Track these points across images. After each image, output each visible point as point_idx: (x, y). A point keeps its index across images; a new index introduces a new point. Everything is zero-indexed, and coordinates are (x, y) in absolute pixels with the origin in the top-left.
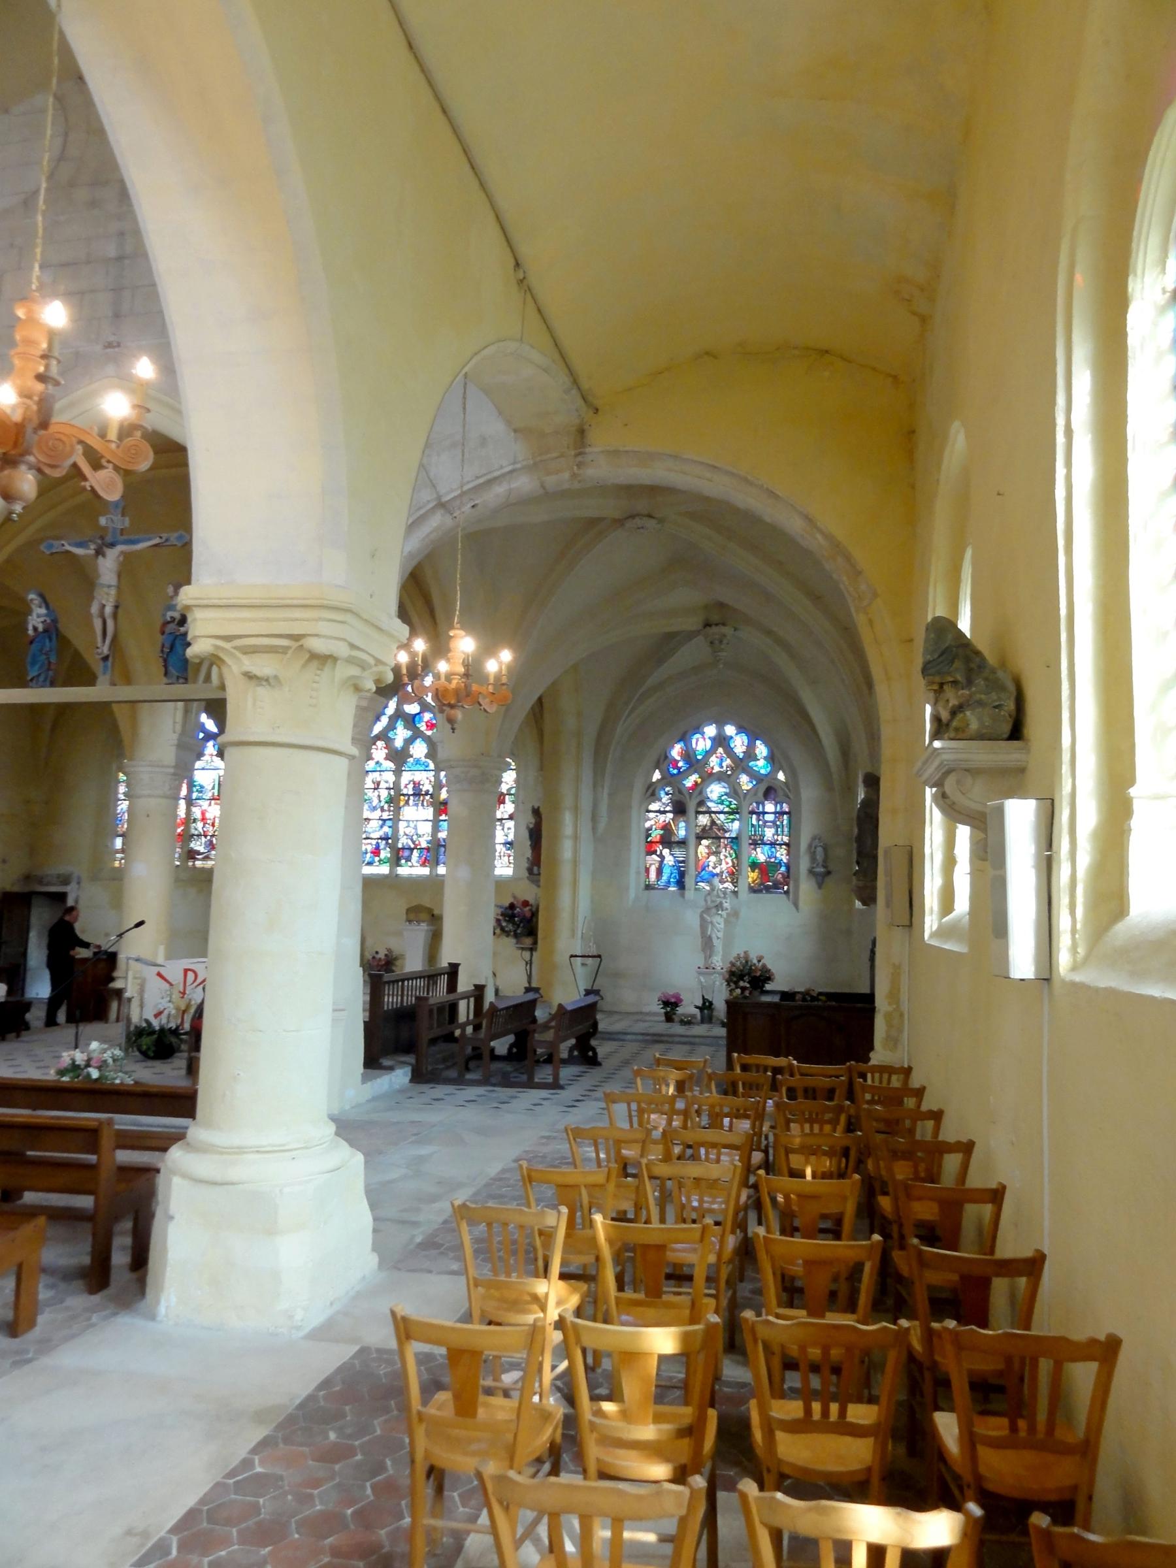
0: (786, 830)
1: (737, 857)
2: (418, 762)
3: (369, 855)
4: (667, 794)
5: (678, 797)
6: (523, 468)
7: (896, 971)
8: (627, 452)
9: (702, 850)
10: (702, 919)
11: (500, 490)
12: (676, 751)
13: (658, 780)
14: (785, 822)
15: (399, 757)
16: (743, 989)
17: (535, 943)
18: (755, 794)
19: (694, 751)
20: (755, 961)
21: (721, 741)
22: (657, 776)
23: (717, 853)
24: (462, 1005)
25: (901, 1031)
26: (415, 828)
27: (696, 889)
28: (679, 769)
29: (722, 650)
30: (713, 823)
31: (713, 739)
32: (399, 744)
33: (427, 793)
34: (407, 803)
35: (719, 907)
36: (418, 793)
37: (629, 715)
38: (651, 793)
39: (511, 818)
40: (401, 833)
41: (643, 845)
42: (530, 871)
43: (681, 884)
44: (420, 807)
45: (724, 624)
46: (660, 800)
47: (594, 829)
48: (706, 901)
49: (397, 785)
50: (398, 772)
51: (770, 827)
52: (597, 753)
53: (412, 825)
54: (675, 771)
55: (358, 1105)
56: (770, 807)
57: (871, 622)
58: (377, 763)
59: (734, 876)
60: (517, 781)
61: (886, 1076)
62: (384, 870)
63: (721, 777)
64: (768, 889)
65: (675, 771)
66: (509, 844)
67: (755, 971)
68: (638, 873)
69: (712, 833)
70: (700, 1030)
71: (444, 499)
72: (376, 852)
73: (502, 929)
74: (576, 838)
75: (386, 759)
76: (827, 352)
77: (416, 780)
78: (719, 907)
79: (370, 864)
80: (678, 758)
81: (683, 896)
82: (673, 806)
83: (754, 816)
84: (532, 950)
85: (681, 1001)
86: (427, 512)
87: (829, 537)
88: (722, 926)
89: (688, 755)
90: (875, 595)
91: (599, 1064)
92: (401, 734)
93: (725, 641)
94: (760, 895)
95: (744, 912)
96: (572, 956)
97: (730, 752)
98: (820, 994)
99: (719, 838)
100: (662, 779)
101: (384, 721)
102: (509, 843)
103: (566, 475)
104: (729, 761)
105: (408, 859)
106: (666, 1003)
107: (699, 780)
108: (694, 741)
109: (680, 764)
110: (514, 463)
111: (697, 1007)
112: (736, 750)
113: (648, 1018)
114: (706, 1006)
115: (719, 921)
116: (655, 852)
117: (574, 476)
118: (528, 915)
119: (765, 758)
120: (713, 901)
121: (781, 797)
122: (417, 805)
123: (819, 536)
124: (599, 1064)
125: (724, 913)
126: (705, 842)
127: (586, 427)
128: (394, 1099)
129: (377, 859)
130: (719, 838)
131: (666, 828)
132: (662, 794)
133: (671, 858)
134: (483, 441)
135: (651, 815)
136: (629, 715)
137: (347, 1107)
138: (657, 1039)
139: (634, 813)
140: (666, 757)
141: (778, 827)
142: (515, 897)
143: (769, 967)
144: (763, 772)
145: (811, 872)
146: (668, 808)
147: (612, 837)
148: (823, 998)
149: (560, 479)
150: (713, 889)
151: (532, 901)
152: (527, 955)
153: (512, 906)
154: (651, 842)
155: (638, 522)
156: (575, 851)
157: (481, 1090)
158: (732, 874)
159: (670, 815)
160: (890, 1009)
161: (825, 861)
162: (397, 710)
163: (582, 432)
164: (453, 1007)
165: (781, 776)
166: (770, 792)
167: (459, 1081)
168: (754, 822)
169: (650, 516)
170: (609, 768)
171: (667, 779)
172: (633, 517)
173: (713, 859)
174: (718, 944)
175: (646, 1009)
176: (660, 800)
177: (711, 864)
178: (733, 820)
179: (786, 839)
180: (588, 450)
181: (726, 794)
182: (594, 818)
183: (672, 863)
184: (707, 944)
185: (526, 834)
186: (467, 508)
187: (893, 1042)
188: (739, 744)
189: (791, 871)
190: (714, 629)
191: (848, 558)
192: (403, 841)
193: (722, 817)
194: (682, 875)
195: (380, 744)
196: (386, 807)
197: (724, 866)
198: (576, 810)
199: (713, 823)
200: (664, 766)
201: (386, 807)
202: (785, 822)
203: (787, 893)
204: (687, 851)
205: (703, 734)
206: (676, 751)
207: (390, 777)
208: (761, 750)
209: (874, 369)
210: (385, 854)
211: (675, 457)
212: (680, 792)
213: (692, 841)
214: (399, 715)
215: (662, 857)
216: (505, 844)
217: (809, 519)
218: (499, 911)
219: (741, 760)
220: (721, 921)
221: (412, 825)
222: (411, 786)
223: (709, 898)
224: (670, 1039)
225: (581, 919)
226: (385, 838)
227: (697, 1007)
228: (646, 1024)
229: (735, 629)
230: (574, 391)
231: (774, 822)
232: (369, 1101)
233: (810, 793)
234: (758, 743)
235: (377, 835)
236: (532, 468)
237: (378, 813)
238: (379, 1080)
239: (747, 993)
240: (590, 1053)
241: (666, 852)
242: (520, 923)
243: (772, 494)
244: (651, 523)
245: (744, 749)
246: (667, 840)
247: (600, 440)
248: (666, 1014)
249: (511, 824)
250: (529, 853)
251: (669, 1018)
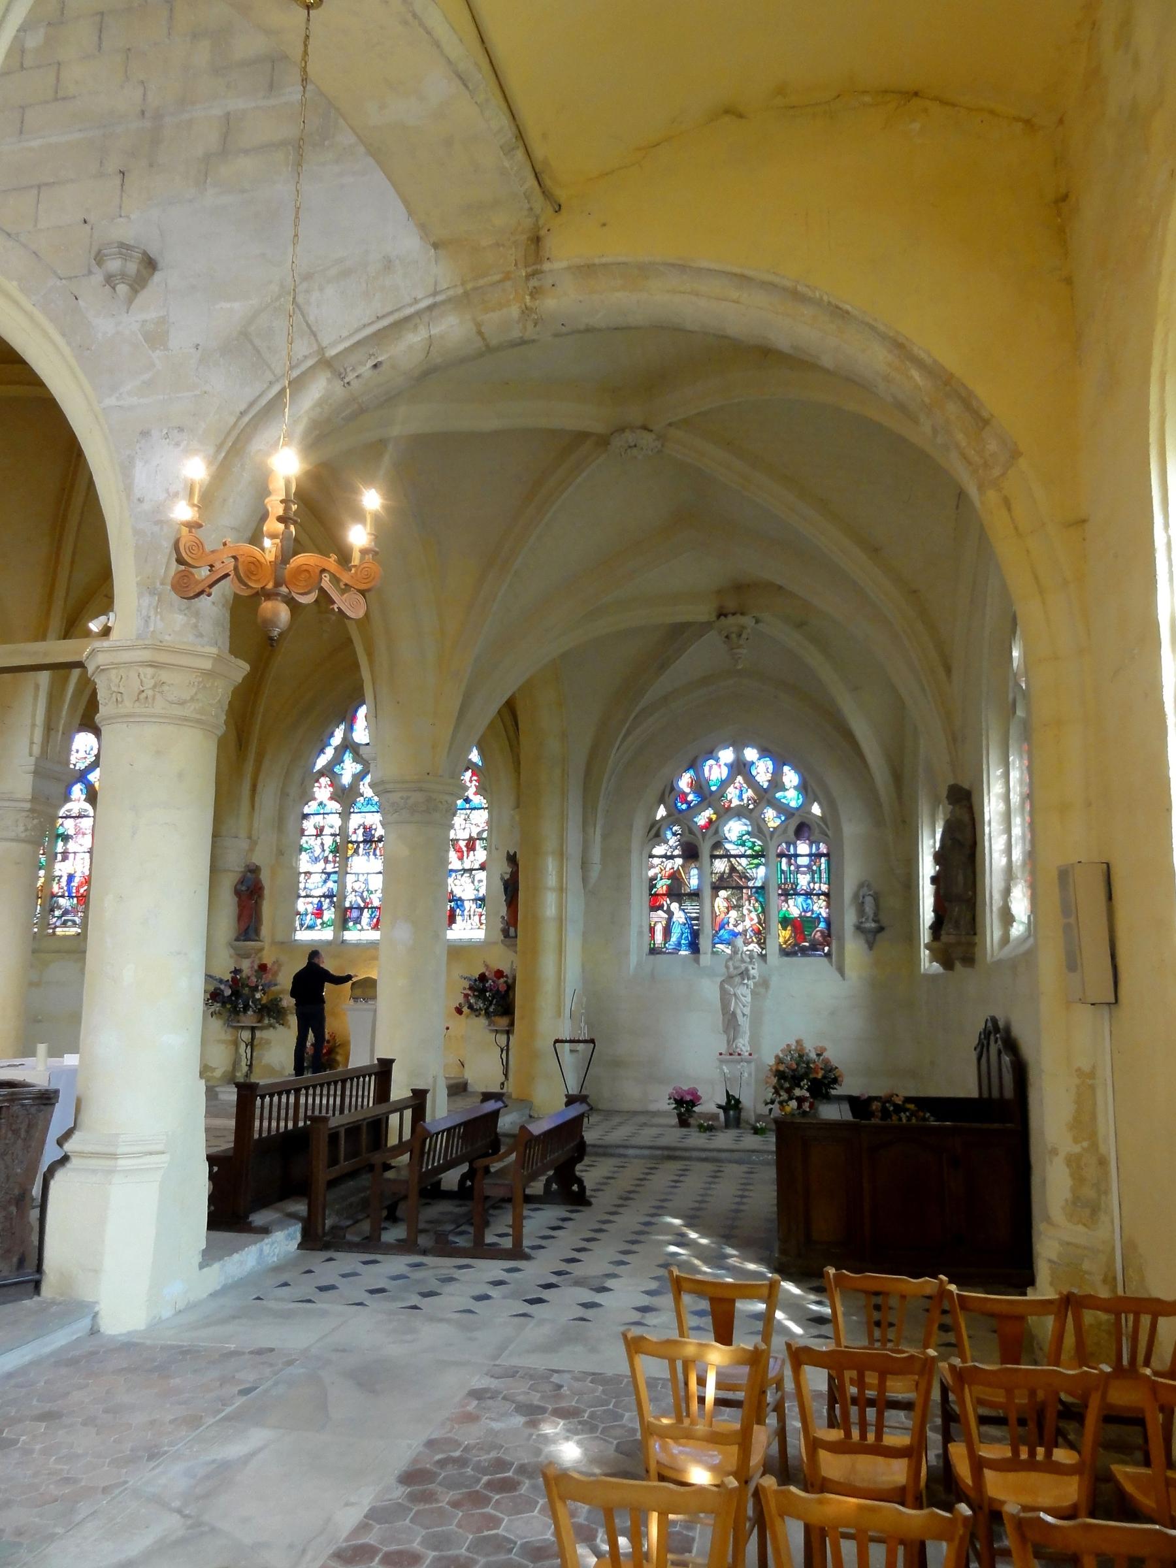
0: (824, 875)
1: (763, 912)
2: (369, 801)
3: (309, 917)
4: (674, 834)
5: (688, 838)
6: (449, 300)
7: (1086, 1084)
8: (605, 265)
9: (720, 903)
10: (723, 991)
11: (415, 338)
12: (684, 782)
13: (663, 818)
14: (823, 866)
15: (346, 797)
16: (800, 1100)
17: (512, 1024)
18: (785, 831)
19: (707, 781)
20: (813, 1055)
21: (740, 768)
22: (662, 812)
23: (738, 907)
24: (394, 1119)
25: (1102, 1189)
26: (366, 882)
27: (713, 953)
28: (689, 803)
29: (739, 647)
30: (733, 869)
31: (730, 766)
32: (346, 780)
33: (380, 840)
34: (356, 852)
35: (744, 974)
36: (369, 840)
37: (625, 737)
38: (655, 834)
39: (482, 867)
40: (349, 889)
41: (646, 898)
42: (506, 933)
43: (694, 947)
44: (372, 857)
45: (742, 614)
46: (666, 842)
47: (585, 880)
48: (727, 967)
49: (343, 830)
50: (345, 815)
51: (804, 873)
52: (586, 789)
53: (362, 878)
54: (684, 807)
55: (191, 1307)
56: (803, 848)
57: (1007, 503)
58: (321, 804)
59: (761, 935)
60: (489, 822)
61: (1146, 1320)
62: (327, 934)
63: (740, 813)
64: (804, 952)
65: (684, 807)
66: (481, 901)
67: (815, 1071)
68: (640, 933)
69: (732, 882)
70: (724, 1139)
71: (331, 352)
72: (319, 913)
73: (471, 1007)
74: (561, 889)
75: (331, 798)
76: (916, 94)
77: (368, 824)
78: (744, 974)
79: (310, 927)
80: (687, 790)
81: (697, 961)
82: (683, 851)
83: (784, 860)
84: (508, 1033)
85: (699, 1098)
86: (304, 374)
87: (934, 372)
88: (749, 999)
89: (700, 786)
90: (1015, 454)
91: (589, 1204)
92: (349, 769)
93: (744, 636)
94: (795, 959)
95: (774, 981)
96: (557, 1041)
97: (751, 781)
98: (908, 1100)
99: (741, 888)
100: (669, 815)
101: (329, 752)
102: (480, 899)
103: (515, 311)
104: (750, 793)
105: (357, 921)
106: (679, 1102)
107: (714, 817)
108: (706, 769)
109: (691, 797)
110: (435, 294)
111: (720, 1107)
112: (758, 778)
113: (656, 1120)
114: (732, 1105)
115: (744, 992)
116: (661, 907)
117: (526, 311)
118: (503, 988)
119: (795, 788)
120: (735, 968)
121: (816, 834)
122: (368, 854)
123: (915, 374)
124: (588, 1204)
125: (751, 983)
126: (723, 893)
127: (543, 233)
128: (251, 1297)
129: (319, 921)
130: (741, 888)
131: (674, 876)
132: (669, 835)
133: (682, 914)
134: (388, 265)
135: (656, 861)
136: (625, 737)
137: (167, 1313)
138: (670, 1154)
139: (635, 857)
140: (672, 789)
141: (813, 872)
142: (487, 966)
143: (834, 1062)
144: (793, 804)
145: (859, 928)
146: (676, 852)
147: (606, 889)
148: (912, 1106)
149: (504, 316)
150: (735, 952)
151: (507, 971)
152: (502, 1039)
153: (483, 978)
154: (656, 895)
155: (629, 436)
156: (561, 906)
157: (397, 1264)
158: (758, 933)
159: (679, 861)
160: (1077, 1149)
161: (876, 914)
162: (345, 739)
163: (537, 240)
164: (378, 1126)
165: (816, 810)
166: (802, 830)
167: (371, 1244)
168: (784, 867)
169: (645, 428)
170: (602, 804)
171: (675, 816)
172: (622, 430)
173: (733, 914)
174: (744, 1023)
175: (653, 1107)
176: (666, 842)
177: (732, 921)
178: (757, 866)
179: (825, 888)
180: (547, 266)
181: (748, 833)
182: (585, 865)
183: (683, 920)
184: (730, 1023)
185: (499, 887)
186: (366, 369)
187: (1088, 1208)
188: (763, 771)
189: (833, 927)
190: (731, 620)
191: (967, 402)
192: (351, 899)
193: (744, 861)
194: (695, 935)
195: (324, 781)
196: (330, 858)
197: (748, 923)
198: (561, 855)
199: (733, 869)
200: (670, 800)
201: (330, 858)
202: (823, 866)
203: (828, 955)
204: (701, 905)
205: (717, 760)
206: (684, 782)
207: (336, 821)
208: (791, 777)
209: (992, 112)
210: (329, 915)
211: (682, 268)
212: (691, 832)
213: (707, 892)
214: (348, 745)
215: (670, 913)
216: (475, 900)
217: (899, 346)
218: (467, 984)
219: (766, 790)
220: (748, 992)
221: (362, 878)
222: (361, 831)
223: (730, 964)
224: (687, 1154)
225: (569, 992)
226: (330, 896)
227: (720, 1107)
228: (654, 1131)
229: (757, 622)
230: (520, 154)
231: (809, 867)
232: (214, 1295)
233: (853, 829)
234: (786, 769)
235: (319, 892)
236: (463, 301)
237: (321, 865)
238: (236, 1256)
239: (806, 1106)
240: (575, 1188)
241: (675, 906)
242: (494, 998)
243: (838, 313)
244: (647, 439)
245: (769, 776)
246: (677, 891)
247: (566, 248)
248: (680, 1115)
249: (482, 875)
250: (503, 910)
251: (683, 1122)
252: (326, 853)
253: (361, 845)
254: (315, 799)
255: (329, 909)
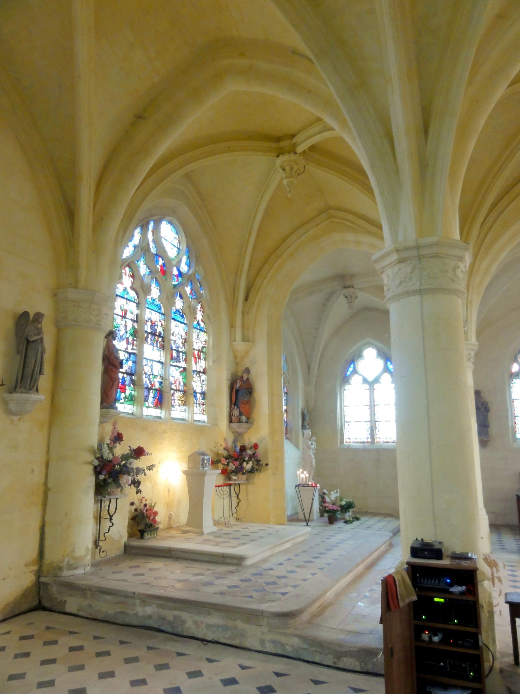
39: (204, 372)
44: (155, 348)
201: (131, 339)
252: (128, 336)
253: (150, 336)
254: (122, 284)
255: (129, 385)
